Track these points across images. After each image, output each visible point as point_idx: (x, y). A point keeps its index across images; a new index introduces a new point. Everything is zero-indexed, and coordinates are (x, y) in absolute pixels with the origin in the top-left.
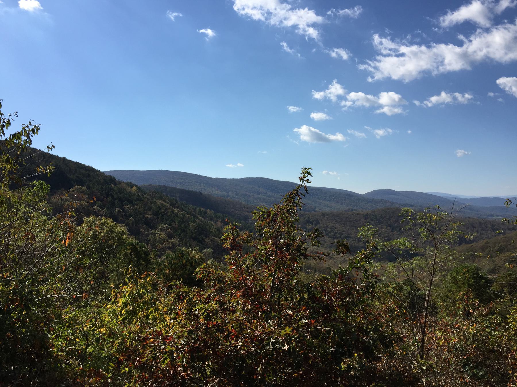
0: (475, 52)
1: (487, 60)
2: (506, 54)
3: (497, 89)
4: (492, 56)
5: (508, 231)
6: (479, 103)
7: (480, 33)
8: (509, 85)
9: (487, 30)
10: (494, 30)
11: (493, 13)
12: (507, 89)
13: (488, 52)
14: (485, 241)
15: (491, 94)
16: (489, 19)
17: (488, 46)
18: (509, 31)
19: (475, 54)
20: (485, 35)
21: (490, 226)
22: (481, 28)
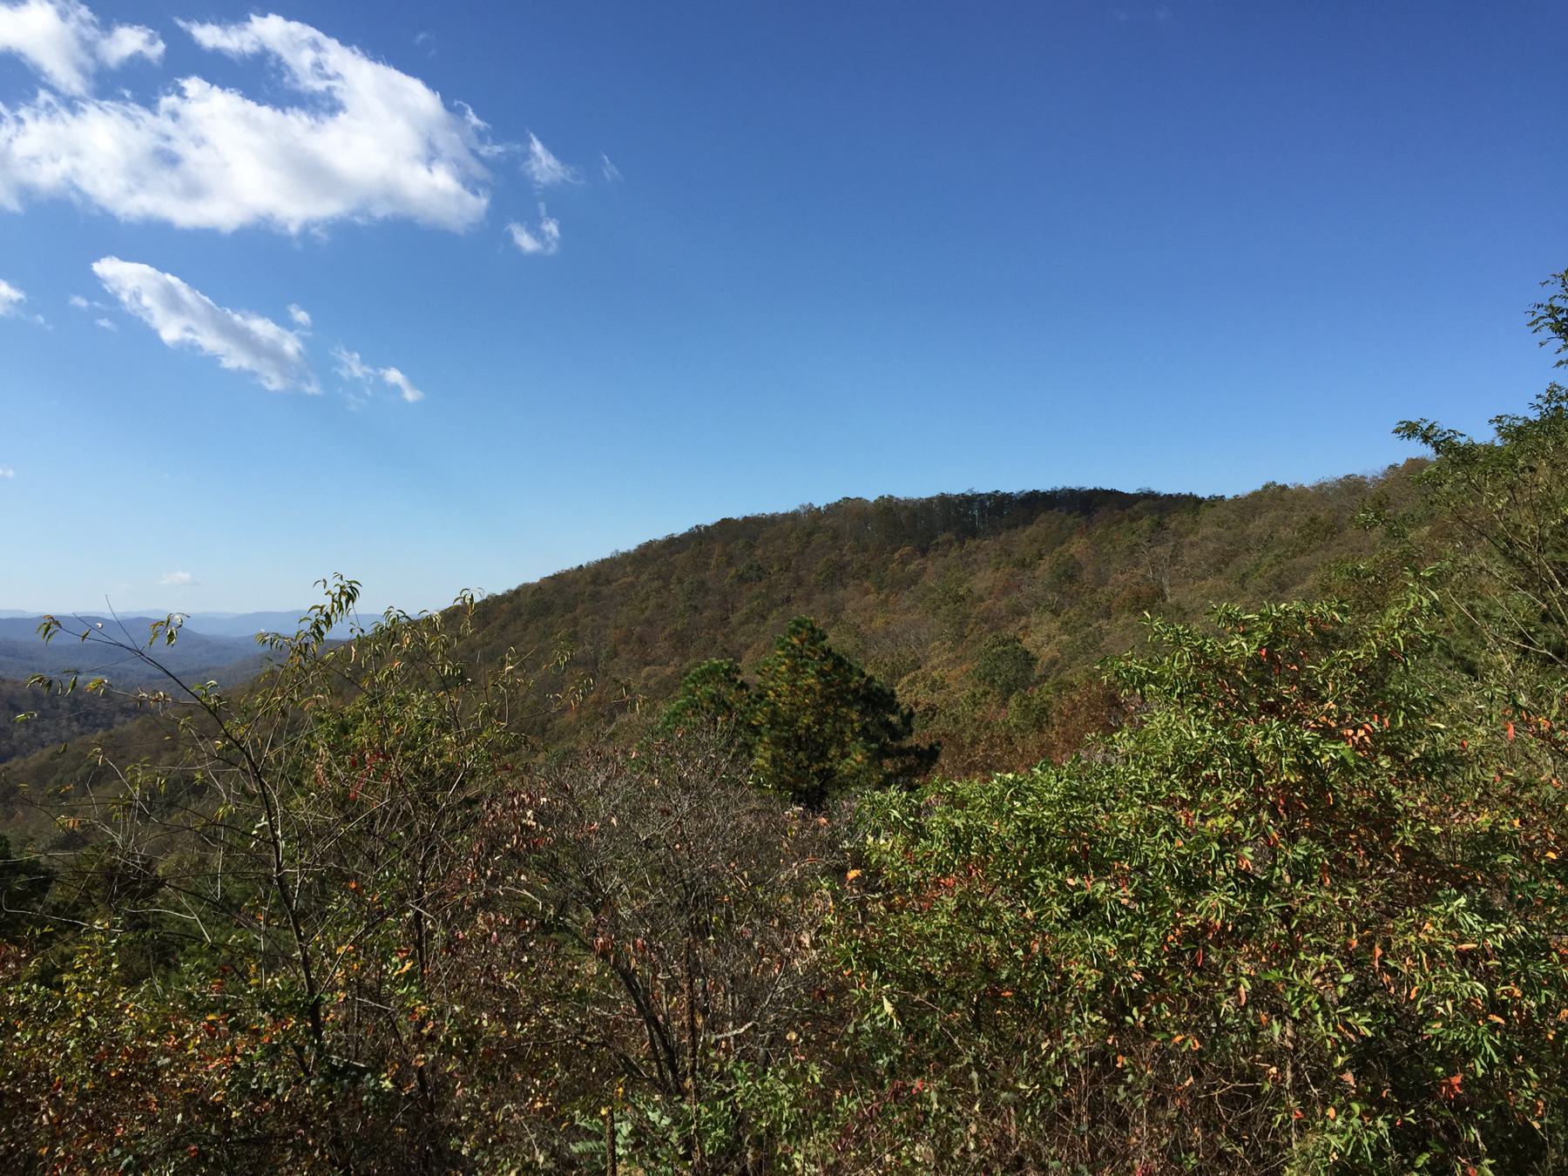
0: (34, 159)
1: (74, 197)
2: (131, 192)
3: (95, 287)
4: (87, 186)
5: (119, 718)
6: (41, 319)
7: (48, 104)
8: (131, 285)
9: (71, 104)
10: (92, 109)
11: (93, 55)
12: (125, 297)
13: (75, 170)
14: (47, 752)
15: (80, 302)
16: (81, 69)
17: (76, 153)
18: (138, 127)
19: (35, 166)
20: (67, 116)
21: (67, 705)
22: (53, 91)
